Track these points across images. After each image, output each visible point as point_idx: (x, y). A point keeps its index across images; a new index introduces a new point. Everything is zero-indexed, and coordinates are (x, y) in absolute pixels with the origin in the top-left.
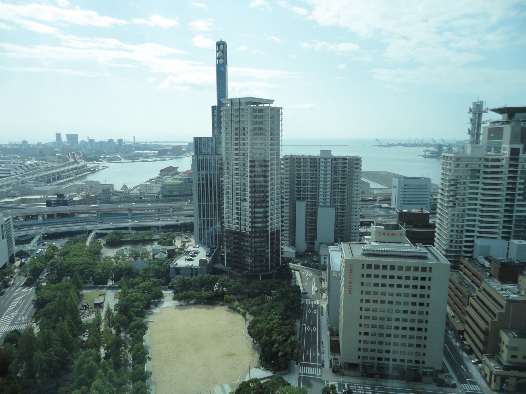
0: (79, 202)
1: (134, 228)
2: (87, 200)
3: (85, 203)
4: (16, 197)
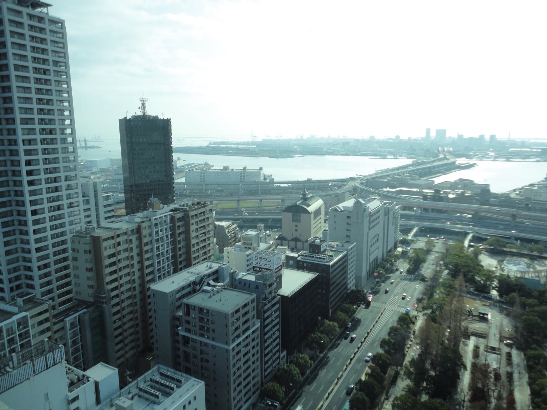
0: (453, 200)
1: (516, 239)
2: (461, 198)
3: (457, 202)
4: (396, 188)
